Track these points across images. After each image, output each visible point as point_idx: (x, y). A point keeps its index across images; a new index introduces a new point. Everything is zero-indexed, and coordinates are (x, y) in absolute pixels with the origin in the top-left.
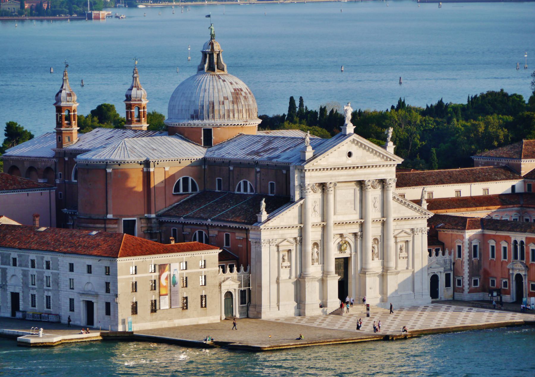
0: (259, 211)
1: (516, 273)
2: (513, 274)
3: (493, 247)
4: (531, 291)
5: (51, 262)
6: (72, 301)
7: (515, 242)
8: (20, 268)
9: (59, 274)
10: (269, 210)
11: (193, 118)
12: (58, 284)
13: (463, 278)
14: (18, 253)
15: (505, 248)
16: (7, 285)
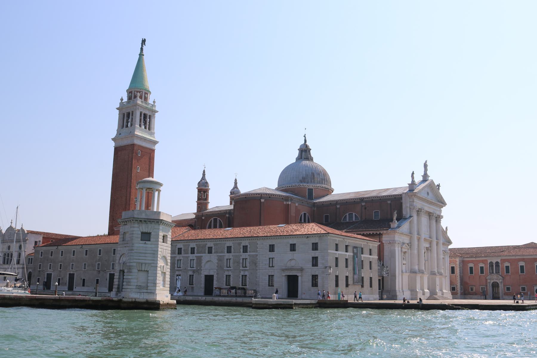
0: (392, 220)
1: (492, 281)
2: (490, 282)
3: (471, 268)
4: (506, 291)
5: (249, 246)
6: (271, 277)
7: (491, 263)
8: (215, 254)
9: (257, 255)
10: (398, 220)
11: (301, 182)
12: (255, 264)
13: (457, 286)
14: (215, 242)
15: (482, 268)
16: (202, 270)
